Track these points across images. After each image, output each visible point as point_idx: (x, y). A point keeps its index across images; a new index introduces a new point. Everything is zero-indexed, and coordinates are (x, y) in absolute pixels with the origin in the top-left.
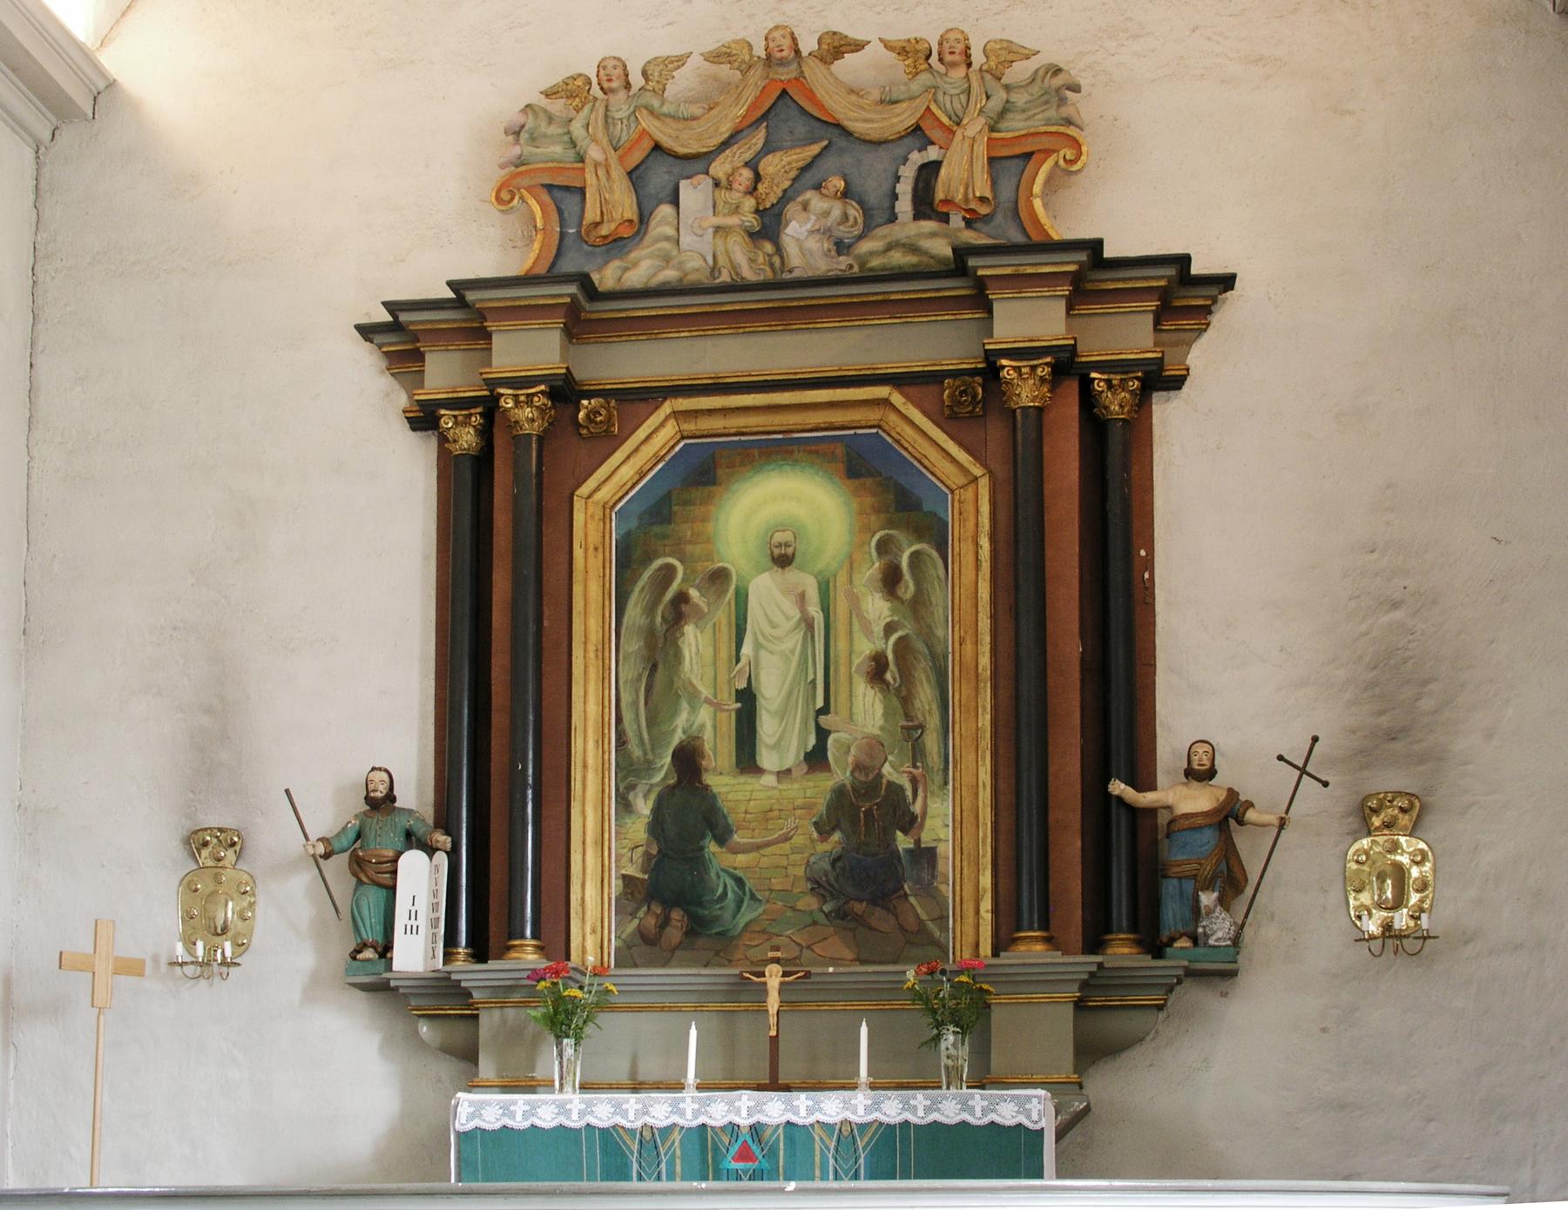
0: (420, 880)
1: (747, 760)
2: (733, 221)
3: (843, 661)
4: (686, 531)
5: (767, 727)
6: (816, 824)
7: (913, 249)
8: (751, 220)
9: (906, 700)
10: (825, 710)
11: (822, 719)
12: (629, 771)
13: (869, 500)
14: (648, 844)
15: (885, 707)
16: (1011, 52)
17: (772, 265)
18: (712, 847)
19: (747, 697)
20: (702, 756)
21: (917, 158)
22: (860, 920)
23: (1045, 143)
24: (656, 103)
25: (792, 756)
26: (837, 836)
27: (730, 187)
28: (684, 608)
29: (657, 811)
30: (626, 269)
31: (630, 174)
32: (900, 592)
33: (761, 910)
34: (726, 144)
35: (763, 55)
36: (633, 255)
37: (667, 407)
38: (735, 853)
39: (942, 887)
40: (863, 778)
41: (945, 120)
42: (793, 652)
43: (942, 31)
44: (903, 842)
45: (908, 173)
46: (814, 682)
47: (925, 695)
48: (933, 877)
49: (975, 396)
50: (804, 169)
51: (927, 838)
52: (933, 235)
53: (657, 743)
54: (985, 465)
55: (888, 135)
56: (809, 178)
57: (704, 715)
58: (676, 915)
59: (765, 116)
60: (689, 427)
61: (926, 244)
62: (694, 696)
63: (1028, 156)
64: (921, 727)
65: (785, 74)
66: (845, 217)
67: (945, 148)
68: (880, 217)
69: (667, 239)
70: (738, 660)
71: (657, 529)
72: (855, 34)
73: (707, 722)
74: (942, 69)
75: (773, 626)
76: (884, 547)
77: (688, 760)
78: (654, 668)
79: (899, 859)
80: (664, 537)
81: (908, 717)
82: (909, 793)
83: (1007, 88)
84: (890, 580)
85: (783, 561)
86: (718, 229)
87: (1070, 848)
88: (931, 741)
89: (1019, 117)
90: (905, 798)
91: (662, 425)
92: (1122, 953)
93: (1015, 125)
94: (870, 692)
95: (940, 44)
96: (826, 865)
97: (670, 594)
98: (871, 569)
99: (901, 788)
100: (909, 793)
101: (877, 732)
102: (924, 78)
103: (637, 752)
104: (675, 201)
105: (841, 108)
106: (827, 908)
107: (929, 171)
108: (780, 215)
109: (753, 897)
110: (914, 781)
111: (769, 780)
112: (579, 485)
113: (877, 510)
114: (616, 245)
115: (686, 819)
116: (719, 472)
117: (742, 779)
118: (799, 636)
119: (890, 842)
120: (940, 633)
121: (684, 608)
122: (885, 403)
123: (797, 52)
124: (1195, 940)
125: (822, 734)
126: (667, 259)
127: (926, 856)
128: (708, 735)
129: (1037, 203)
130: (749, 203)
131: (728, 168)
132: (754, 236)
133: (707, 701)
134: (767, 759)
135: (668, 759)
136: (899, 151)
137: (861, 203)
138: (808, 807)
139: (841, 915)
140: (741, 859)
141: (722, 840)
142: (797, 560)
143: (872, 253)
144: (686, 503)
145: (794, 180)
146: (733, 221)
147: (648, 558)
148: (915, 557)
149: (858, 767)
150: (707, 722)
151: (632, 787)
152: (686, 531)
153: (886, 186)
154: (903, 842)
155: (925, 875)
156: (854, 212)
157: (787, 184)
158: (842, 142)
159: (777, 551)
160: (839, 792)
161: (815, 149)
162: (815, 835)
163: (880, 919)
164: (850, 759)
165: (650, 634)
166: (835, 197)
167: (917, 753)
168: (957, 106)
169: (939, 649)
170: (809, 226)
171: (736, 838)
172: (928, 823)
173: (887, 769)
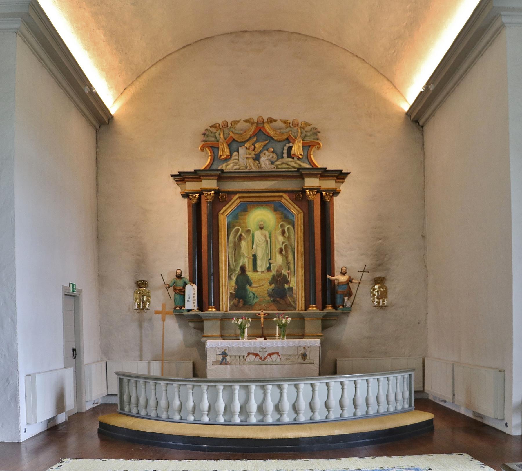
0: (191, 291)
1: (255, 269)
4: (241, 221)
5: (259, 262)
7: (287, 164)
9: (287, 257)
10: (270, 259)
12: (231, 271)
13: (279, 216)
16: (307, 124)
18: (248, 287)
19: (255, 256)
21: (288, 145)
22: (278, 302)
23: (314, 144)
24: (234, 130)
25: (264, 268)
26: (273, 285)
27: (249, 149)
29: (237, 279)
31: (228, 145)
32: (285, 235)
36: (229, 162)
37: (237, 196)
44: (286, 286)
45: (286, 148)
47: (290, 257)
50: (264, 146)
51: (291, 286)
52: (291, 161)
53: (237, 265)
56: (265, 148)
57: (246, 260)
58: (241, 300)
59: (256, 134)
60: (242, 200)
61: (290, 163)
62: (244, 255)
63: (310, 146)
65: (260, 126)
66: (273, 157)
67: (293, 143)
68: (280, 157)
69: (236, 159)
71: (235, 221)
74: (292, 126)
77: (243, 269)
78: (236, 249)
80: (237, 222)
81: (287, 261)
83: (306, 131)
84: (283, 233)
85: (261, 228)
86: (247, 158)
88: (292, 266)
92: (329, 309)
93: (308, 139)
94: (279, 256)
98: (280, 230)
102: (289, 129)
103: (232, 267)
104: (238, 151)
105: (271, 133)
107: (290, 148)
108: (259, 156)
111: (259, 273)
112: (220, 211)
113: (280, 218)
115: (243, 281)
116: (248, 209)
118: (265, 244)
119: (284, 286)
120: (293, 244)
122: (281, 196)
124: (343, 306)
125: (270, 264)
126: (237, 163)
127: (291, 289)
128: (247, 264)
129: (312, 156)
130: (254, 153)
131: (249, 145)
134: (259, 269)
135: (239, 269)
136: (284, 143)
137: (276, 154)
140: (254, 289)
143: (279, 165)
144: (241, 215)
147: (234, 227)
148: (288, 228)
149: (277, 271)
150: (246, 261)
151: (231, 274)
152: (241, 221)
153: (281, 151)
154: (286, 286)
155: (291, 293)
156: (275, 156)
158: (272, 141)
160: (274, 276)
161: (267, 142)
163: (282, 302)
165: (235, 243)
167: (289, 268)
171: (253, 285)
173: (283, 271)
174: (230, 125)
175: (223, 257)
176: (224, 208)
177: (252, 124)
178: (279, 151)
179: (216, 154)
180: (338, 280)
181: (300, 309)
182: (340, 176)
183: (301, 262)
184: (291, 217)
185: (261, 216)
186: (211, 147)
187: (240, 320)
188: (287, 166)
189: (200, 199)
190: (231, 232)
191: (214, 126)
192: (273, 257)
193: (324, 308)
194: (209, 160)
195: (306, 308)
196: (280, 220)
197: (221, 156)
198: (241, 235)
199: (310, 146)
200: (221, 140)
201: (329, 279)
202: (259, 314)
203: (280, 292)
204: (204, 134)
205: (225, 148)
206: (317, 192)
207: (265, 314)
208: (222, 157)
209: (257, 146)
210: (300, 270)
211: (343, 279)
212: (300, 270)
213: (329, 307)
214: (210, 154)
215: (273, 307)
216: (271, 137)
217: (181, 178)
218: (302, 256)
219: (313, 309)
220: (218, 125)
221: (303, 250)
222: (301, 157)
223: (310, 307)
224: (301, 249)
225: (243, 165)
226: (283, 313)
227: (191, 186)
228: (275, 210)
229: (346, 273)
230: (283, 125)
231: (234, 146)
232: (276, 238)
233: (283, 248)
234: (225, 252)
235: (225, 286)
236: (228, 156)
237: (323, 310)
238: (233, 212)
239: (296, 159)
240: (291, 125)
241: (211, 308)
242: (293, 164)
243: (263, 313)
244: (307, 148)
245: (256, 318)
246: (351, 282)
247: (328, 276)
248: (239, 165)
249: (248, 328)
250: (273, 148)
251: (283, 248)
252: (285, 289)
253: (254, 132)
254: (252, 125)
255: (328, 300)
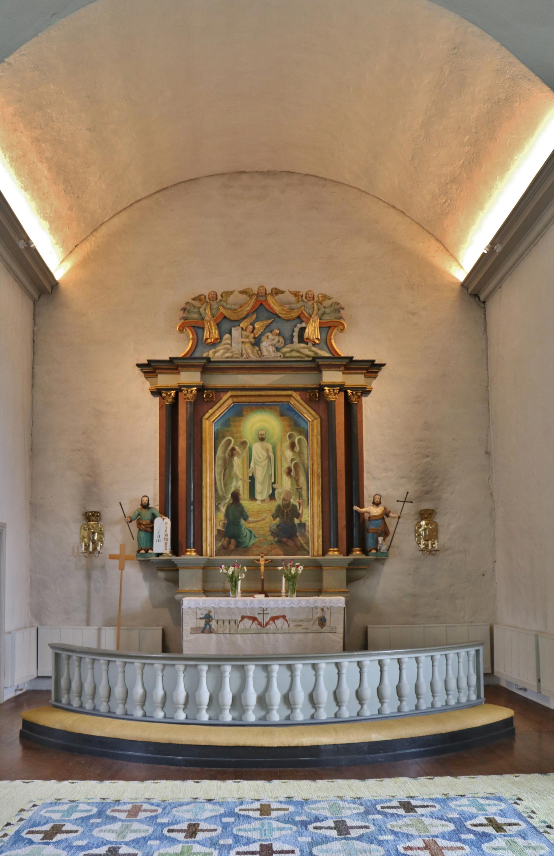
1: (252, 497)
2: (247, 340)
3: (279, 468)
4: (234, 429)
5: (258, 487)
6: (272, 516)
7: (298, 352)
8: (252, 340)
9: (297, 481)
10: (274, 483)
11: (274, 485)
12: (218, 499)
13: (286, 423)
14: (225, 520)
15: (291, 483)
17: (258, 354)
18: (242, 521)
19: (252, 479)
20: (240, 495)
21: (299, 326)
22: (285, 544)
23: (335, 324)
24: (225, 304)
25: (265, 495)
26: (278, 519)
27: (246, 330)
28: (234, 452)
29: (227, 510)
30: (215, 352)
31: (217, 324)
32: (295, 449)
33: (257, 540)
34: (244, 318)
35: (256, 293)
36: (218, 348)
37: (229, 394)
38: (249, 523)
39: (307, 534)
40: (285, 502)
41: (307, 315)
42: (265, 465)
43: (307, 291)
44: (297, 521)
45: (297, 330)
46: (271, 475)
47: (302, 480)
48: (305, 531)
49: (316, 395)
50: (267, 326)
51: (303, 520)
52: (304, 348)
53: (226, 491)
54: (319, 415)
55: (291, 318)
56: (268, 329)
57: (240, 483)
58: (233, 541)
59: (256, 310)
60: (235, 400)
61: (302, 350)
62: (237, 477)
63: (330, 327)
64: (301, 488)
66: (279, 341)
67: (307, 323)
68: (288, 341)
69: (228, 344)
70: (250, 468)
71: (226, 429)
72: (281, 288)
73: (239, 484)
75: (260, 458)
76: (290, 436)
77: (236, 496)
78: (225, 469)
79: (295, 526)
80: (228, 431)
81: (298, 485)
82: (298, 507)
83: (324, 307)
84: (292, 446)
85: (262, 439)
86: (243, 342)
87: (342, 522)
88: (304, 493)
89: (327, 316)
90: (297, 508)
91: (228, 399)
93: (327, 318)
94: (287, 478)
95: (306, 294)
96: (275, 527)
97: (230, 448)
98: (287, 443)
99: (296, 506)
100: (298, 507)
101: (289, 489)
102: (301, 303)
103: (221, 493)
104: (230, 333)
105: (277, 309)
106: (276, 539)
107: (303, 330)
108: (260, 339)
109: (255, 536)
110: (299, 504)
111: (259, 502)
113: (289, 426)
114: (214, 344)
115: (236, 512)
116: (244, 413)
117: (251, 502)
118: (267, 461)
120: (306, 462)
121: (234, 452)
122: (290, 396)
123: (266, 294)
125: (274, 490)
127: (303, 525)
128: (241, 489)
129: (333, 341)
130: (252, 335)
131: (246, 324)
132: (253, 345)
133: (241, 479)
134: (258, 496)
135: (230, 496)
136: (294, 323)
138: (270, 510)
139: (279, 542)
140: (251, 525)
141: (246, 519)
142: (266, 439)
143: (287, 352)
144: (234, 421)
145: (265, 329)
146: (247, 340)
147: (223, 437)
148: (299, 440)
149: (284, 499)
150: (239, 484)
151: (219, 504)
152: (234, 429)
153: (290, 333)
154: (297, 521)
155: (303, 531)
156: (281, 340)
157: (262, 330)
158: (278, 319)
159: (260, 437)
160: (279, 507)
161: (270, 321)
162: (272, 519)
163: (290, 543)
164: (282, 497)
165: (224, 460)
166: (276, 335)
167: (300, 496)
168: (311, 312)
169: (306, 466)
170: (269, 343)
171: (250, 519)
172: (304, 516)
173: (292, 500)
174: (219, 298)
175: (207, 479)
176: (211, 411)
177: (251, 296)
178: (287, 334)
179: (200, 337)
180: (369, 513)
181: (315, 554)
182: (372, 368)
183: (317, 488)
184: (303, 424)
185: (261, 422)
186: (194, 327)
187: (231, 569)
188: (298, 354)
189: (176, 397)
190: (219, 444)
191: (198, 298)
192: (278, 480)
193: (349, 552)
194: (190, 344)
195: (324, 553)
196: (288, 429)
197: (207, 339)
198: (233, 449)
199: (330, 327)
200: (207, 318)
201: (356, 511)
202: (258, 560)
203: (287, 530)
204: (184, 309)
205: (213, 328)
206: (340, 390)
207: (266, 560)
208: (209, 341)
209: (257, 326)
210: (316, 498)
211: (376, 511)
212: (316, 498)
213: (356, 551)
214: (191, 337)
215: (278, 550)
216: (276, 315)
217: (150, 368)
218: (318, 479)
219: (334, 554)
220: (203, 297)
221: (320, 470)
222: (317, 342)
223: (329, 551)
224: (317, 468)
225: (237, 352)
226: (293, 560)
227: (165, 380)
228: (282, 415)
229: (380, 503)
230: (293, 299)
231: (226, 325)
232: (283, 452)
233: (293, 468)
234: (211, 472)
235: (211, 520)
236: (217, 339)
237: (347, 555)
238: (222, 417)
239: (310, 344)
240: (304, 298)
241: (190, 551)
242: (307, 351)
243: (263, 559)
244: (326, 330)
245: (253, 566)
246: (388, 516)
247: (356, 508)
248: (232, 352)
249: (242, 580)
250: (279, 329)
251: (293, 468)
252: (294, 524)
253: (253, 307)
254: (251, 298)
255: (355, 541)
